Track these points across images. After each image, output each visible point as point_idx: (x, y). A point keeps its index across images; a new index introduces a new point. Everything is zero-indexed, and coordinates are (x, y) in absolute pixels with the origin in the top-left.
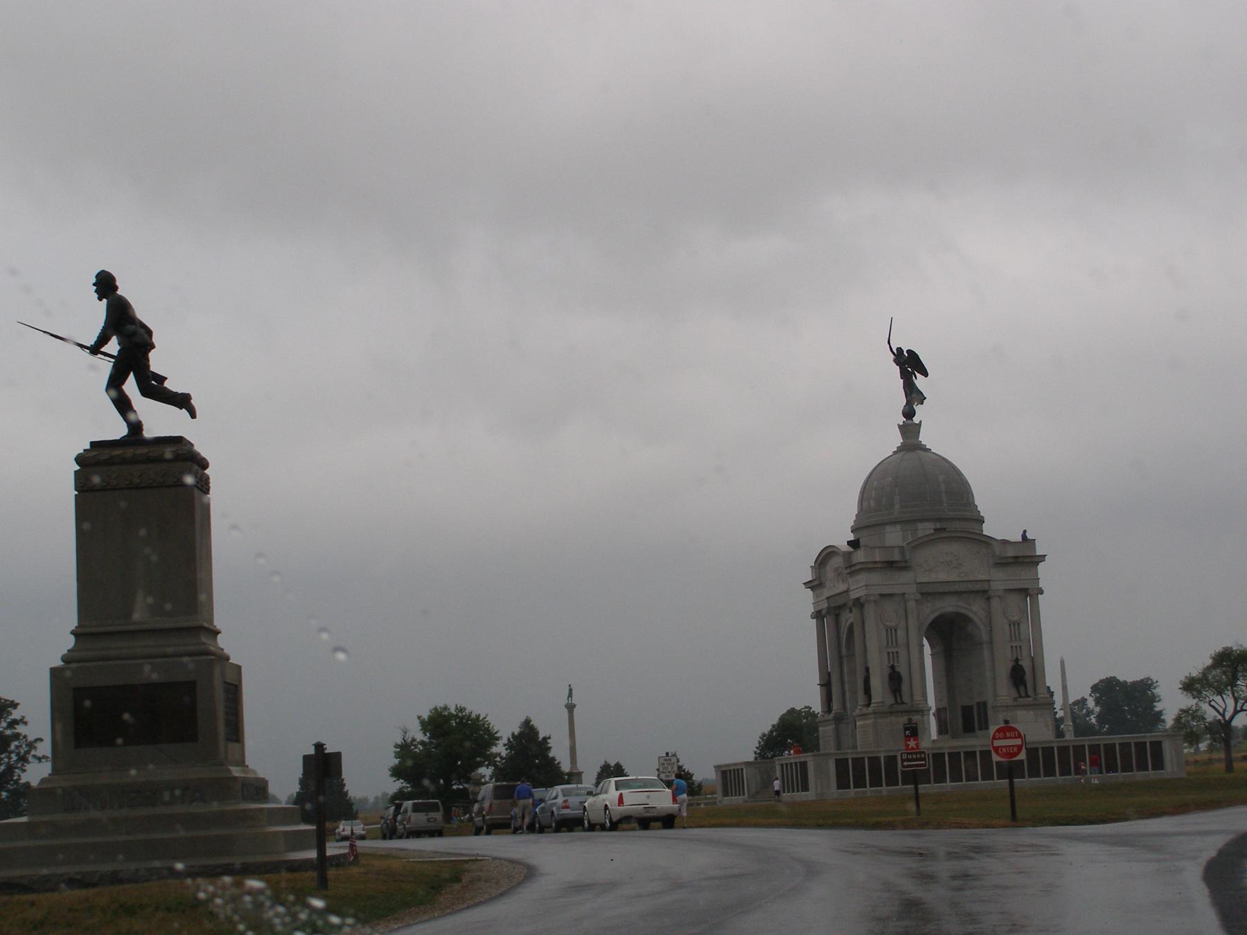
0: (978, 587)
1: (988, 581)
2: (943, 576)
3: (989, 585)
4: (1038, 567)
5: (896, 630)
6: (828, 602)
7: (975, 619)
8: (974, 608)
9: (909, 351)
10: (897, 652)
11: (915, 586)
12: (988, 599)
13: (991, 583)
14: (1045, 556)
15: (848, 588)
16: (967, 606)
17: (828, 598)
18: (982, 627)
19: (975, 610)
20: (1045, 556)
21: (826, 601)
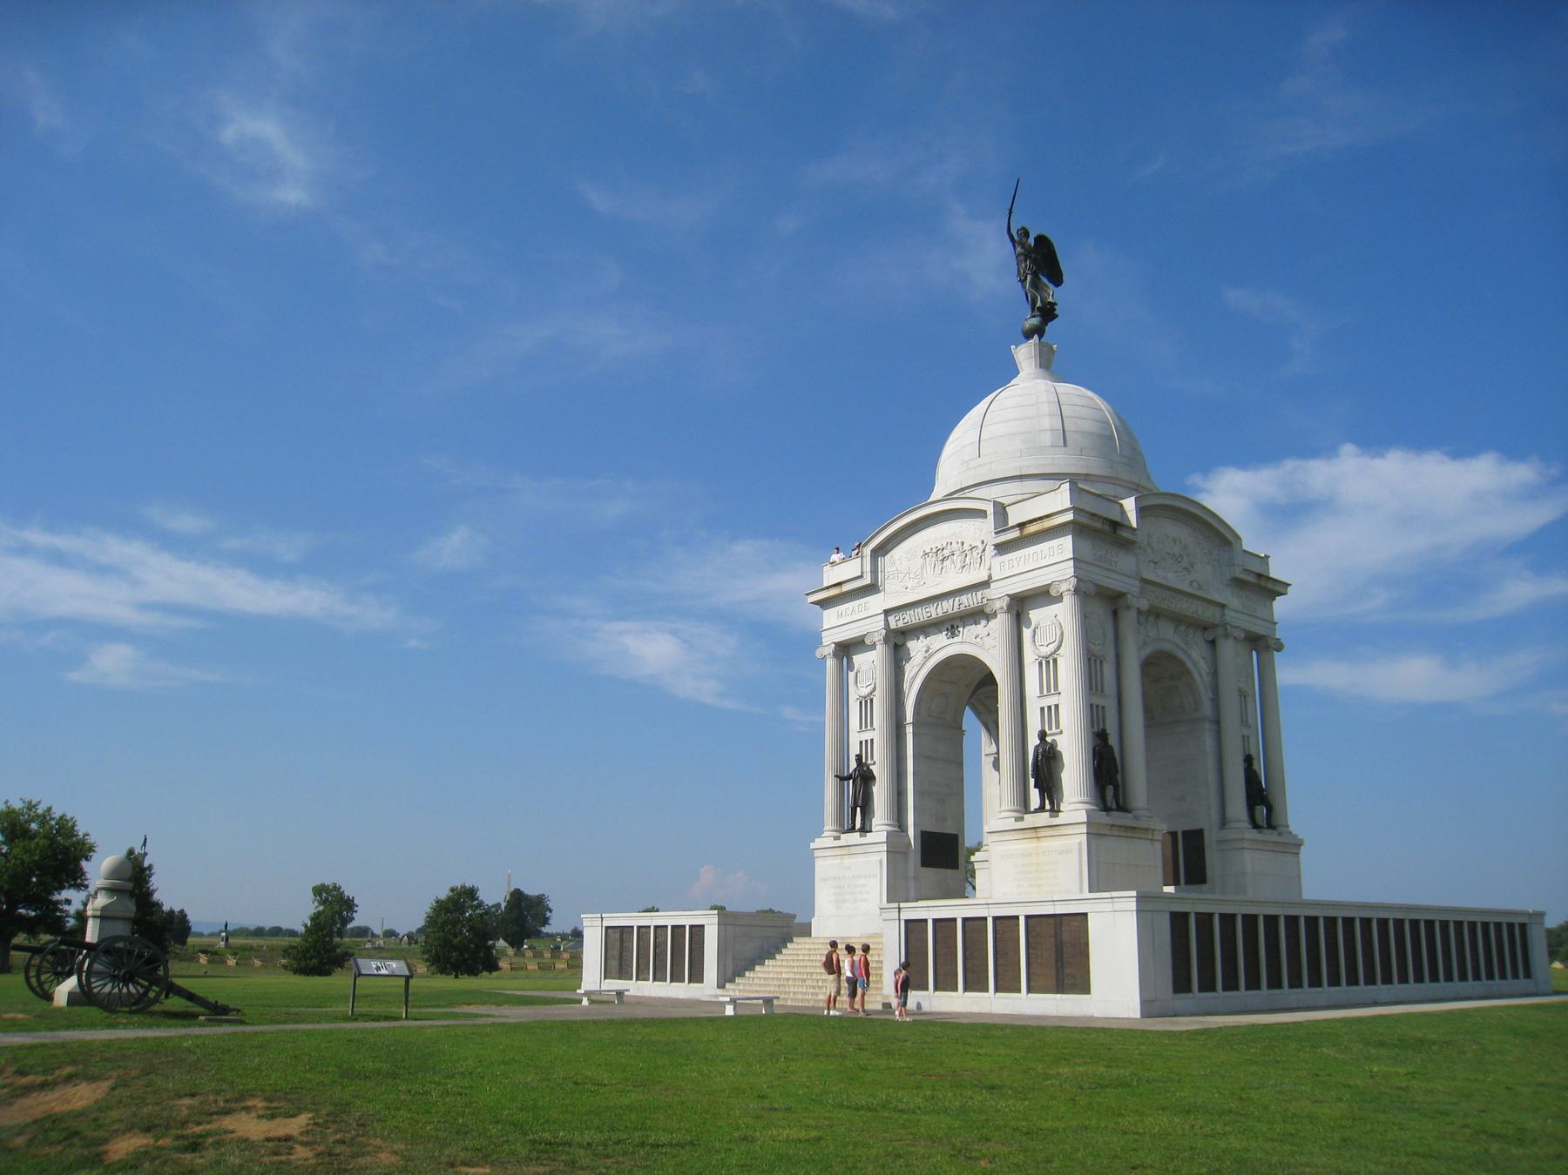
0: (1209, 614)
1: (1223, 606)
2: (1172, 578)
3: (1223, 615)
4: (1274, 603)
5: (1101, 662)
6: (886, 621)
7: (1194, 672)
8: (1196, 655)
9: (1042, 241)
10: (1103, 707)
11: (1137, 583)
12: (1213, 643)
13: (1227, 612)
14: (1290, 585)
15: (990, 577)
16: (1185, 647)
17: (887, 612)
18: (1202, 690)
19: (1195, 656)
20: (1290, 585)
21: (883, 615)
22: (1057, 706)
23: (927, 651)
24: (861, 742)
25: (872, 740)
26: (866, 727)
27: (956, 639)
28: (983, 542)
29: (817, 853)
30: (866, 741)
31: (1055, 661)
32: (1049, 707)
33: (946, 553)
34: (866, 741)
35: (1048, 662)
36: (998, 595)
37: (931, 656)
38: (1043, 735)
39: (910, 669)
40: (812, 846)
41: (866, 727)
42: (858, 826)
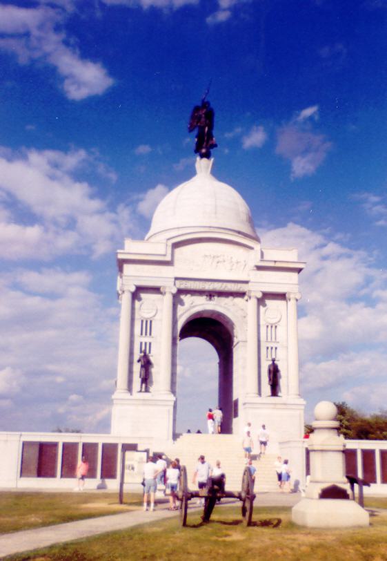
22: (276, 348)
23: (192, 304)
24: (141, 343)
25: (150, 344)
26: (146, 334)
27: (211, 302)
28: (245, 261)
29: (115, 402)
30: (146, 343)
31: (276, 327)
32: (272, 348)
33: (221, 259)
34: (146, 343)
35: (272, 327)
36: (256, 290)
37: (194, 307)
38: (273, 360)
39: (180, 309)
40: (113, 397)
41: (146, 334)
42: (143, 390)
